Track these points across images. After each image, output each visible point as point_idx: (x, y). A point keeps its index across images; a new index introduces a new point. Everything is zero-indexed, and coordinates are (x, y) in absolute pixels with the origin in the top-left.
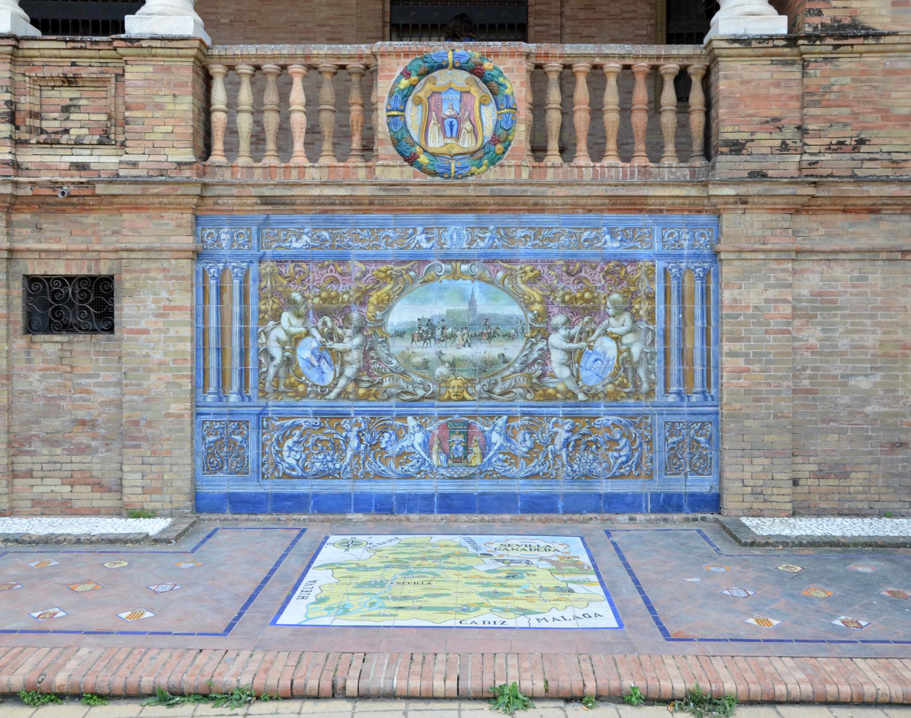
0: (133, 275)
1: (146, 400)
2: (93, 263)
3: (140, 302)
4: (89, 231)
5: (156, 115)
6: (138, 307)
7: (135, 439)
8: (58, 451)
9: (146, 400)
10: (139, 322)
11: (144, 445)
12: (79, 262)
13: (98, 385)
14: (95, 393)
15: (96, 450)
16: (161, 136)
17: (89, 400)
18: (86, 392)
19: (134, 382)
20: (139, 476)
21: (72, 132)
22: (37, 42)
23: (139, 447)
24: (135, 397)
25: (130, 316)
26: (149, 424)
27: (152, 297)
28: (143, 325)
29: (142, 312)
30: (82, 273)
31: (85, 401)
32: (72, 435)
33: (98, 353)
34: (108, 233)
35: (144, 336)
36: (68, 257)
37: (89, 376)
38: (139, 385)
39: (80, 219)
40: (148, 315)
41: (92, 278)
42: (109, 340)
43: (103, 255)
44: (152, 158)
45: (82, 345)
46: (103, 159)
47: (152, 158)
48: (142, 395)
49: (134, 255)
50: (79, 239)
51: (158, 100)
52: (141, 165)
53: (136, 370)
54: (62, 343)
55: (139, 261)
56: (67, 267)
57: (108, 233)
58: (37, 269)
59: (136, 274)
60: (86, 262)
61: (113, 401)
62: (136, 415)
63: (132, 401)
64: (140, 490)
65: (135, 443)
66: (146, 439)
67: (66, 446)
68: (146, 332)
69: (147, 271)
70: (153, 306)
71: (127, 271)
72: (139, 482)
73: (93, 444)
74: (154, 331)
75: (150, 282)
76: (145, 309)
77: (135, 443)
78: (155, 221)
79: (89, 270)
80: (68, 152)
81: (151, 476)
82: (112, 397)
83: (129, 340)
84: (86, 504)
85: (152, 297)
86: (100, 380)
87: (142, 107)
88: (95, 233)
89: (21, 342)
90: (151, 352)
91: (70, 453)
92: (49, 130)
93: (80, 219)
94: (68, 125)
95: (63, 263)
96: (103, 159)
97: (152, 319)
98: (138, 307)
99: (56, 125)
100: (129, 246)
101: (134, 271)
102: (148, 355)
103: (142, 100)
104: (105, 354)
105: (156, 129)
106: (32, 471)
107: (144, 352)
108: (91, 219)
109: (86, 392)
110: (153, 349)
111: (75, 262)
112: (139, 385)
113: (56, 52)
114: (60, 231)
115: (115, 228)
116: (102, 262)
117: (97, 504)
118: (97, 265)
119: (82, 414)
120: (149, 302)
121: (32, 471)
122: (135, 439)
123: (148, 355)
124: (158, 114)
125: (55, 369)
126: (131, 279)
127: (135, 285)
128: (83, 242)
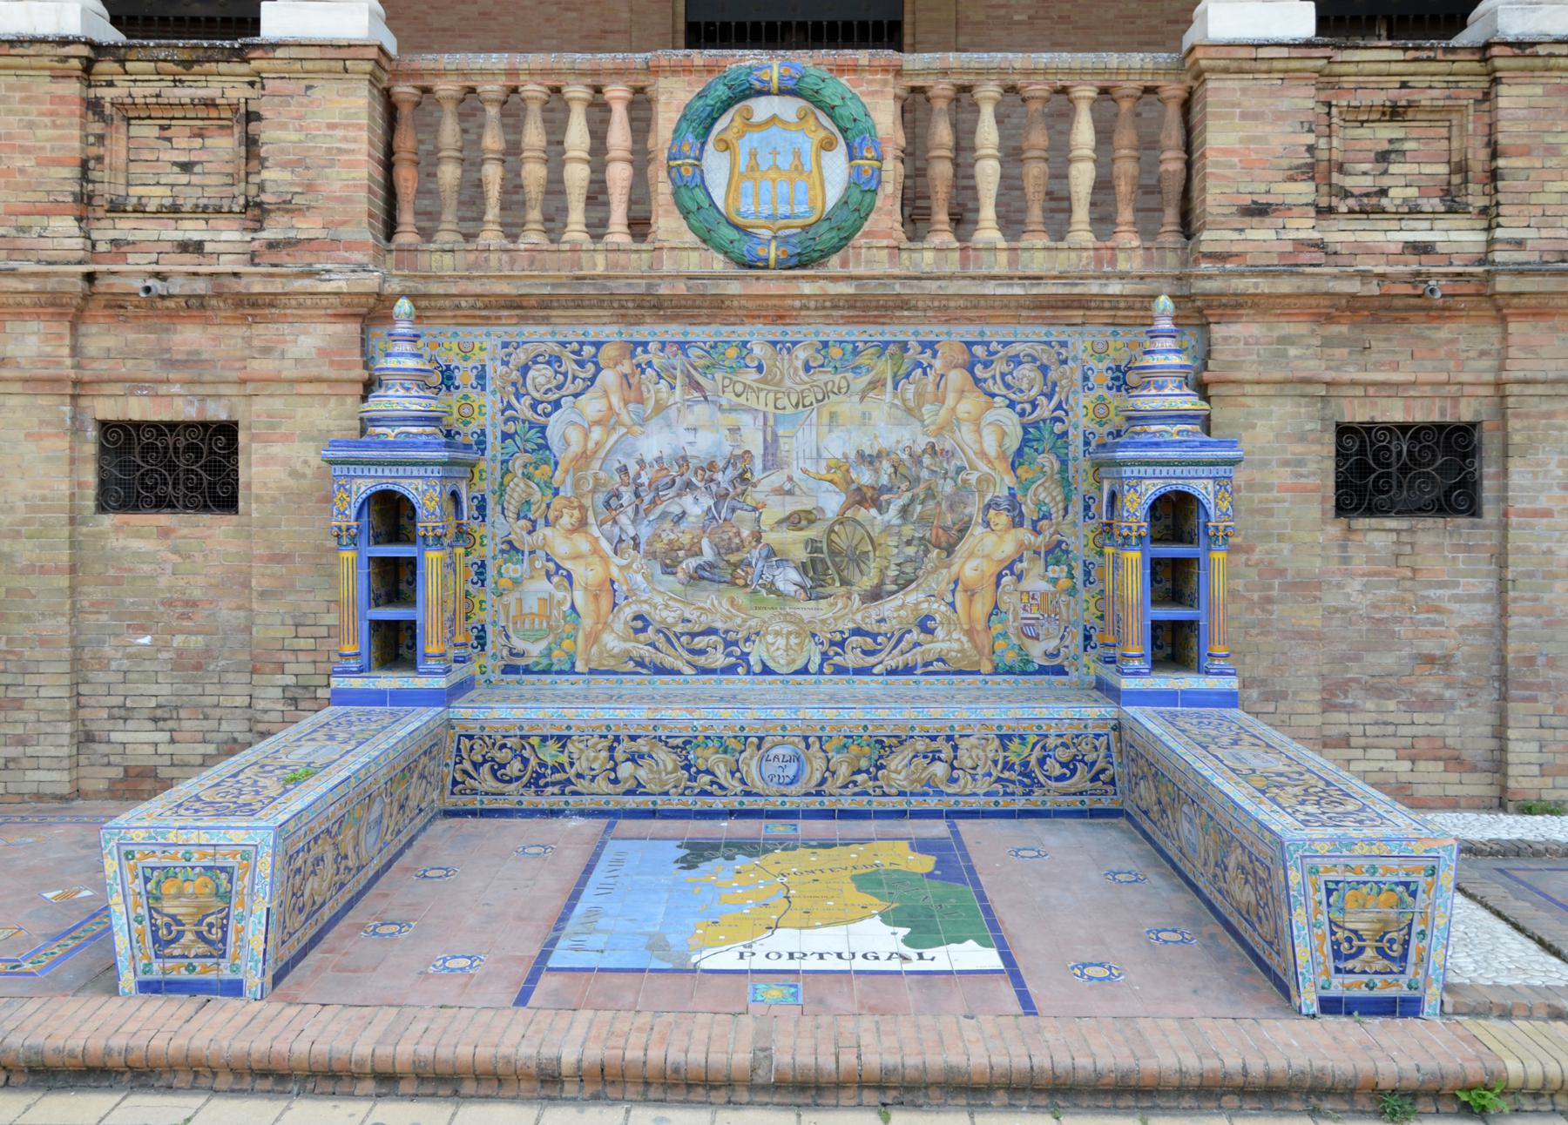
0: (1526, 422)
1: (1548, 624)
2: (1449, 403)
3: (1538, 465)
4: (1442, 352)
5: (1549, 164)
6: (1535, 474)
7: (1527, 686)
8: (1391, 705)
9: (1548, 624)
10: (1536, 499)
11: (1544, 696)
12: (1426, 401)
13: (1457, 599)
14: (1451, 612)
15: (1451, 705)
16: (1556, 198)
17: (1442, 624)
18: (1438, 610)
19: (1529, 595)
20: (1535, 746)
21: (1392, 193)
22: (1358, 52)
23: (1534, 699)
24: (1528, 620)
25: (1523, 488)
26: (1552, 663)
27: (1556, 458)
28: (1543, 503)
29: (1541, 481)
30: (1430, 419)
31: (1435, 624)
32: (1413, 679)
33: (1456, 548)
34: (1472, 354)
35: (1545, 521)
36: (1412, 393)
37: (1442, 585)
38: (1535, 600)
39: (1428, 333)
40: (1551, 487)
41: (1440, 427)
42: (1474, 526)
43: (1468, 390)
44: (1544, 233)
45: (1433, 539)
46: (1454, 236)
47: (1544, 233)
48: (1540, 616)
49: (1530, 390)
50: (1428, 364)
51: (1550, 139)
52: (1529, 244)
53: (1530, 575)
54: (1398, 532)
55: (1536, 399)
56: (1407, 409)
57: (1472, 354)
58: (1358, 414)
59: (1532, 421)
60: (1438, 402)
61: (1479, 625)
62: (1530, 648)
63: (1524, 625)
64: (1535, 770)
65: (1527, 693)
66: (1545, 686)
67: (1404, 697)
68: (1547, 513)
69: (1549, 415)
70: (1560, 472)
71: (1517, 416)
72: (1535, 757)
73: (1448, 694)
74: (1561, 512)
75: (1555, 433)
76: (1545, 476)
77: (1527, 693)
78: (1562, 335)
79: (1443, 414)
80: (1394, 225)
81: (1554, 748)
82: (1478, 619)
83: (1520, 527)
84: (1436, 791)
85: (1556, 458)
86: (1459, 591)
87: (1526, 152)
88: (1451, 355)
89: (1335, 529)
90: (1555, 547)
91: (1410, 708)
92: (1356, 191)
93: (1428, 333)
94: (1385, 182)
95: (1399, 403)
96: (1454, 236)
97: (1557, 492)
98: (1535, 474)
99: (1367, 182)
100: (1530, 375)
101: (1527, 416)
102: (1550, 552)
103: (1526, 141)
104: (1468, 548)
105: (1549, 187)
106: (1348, 736)
107: (1544, 546)
108: (1445, 331)
109: (1438, 610)
110: (1559, 541)
111: (1420, 401)
112: (1535, 600)
113: (1384, 67)
114: (1395, 352)
115: (1484, 347)
116: (1463, 401)
117: (1452, 791)
118: (1455, 406)
119: (1429, 647)
120: (1552, 466)
121: (1348, 736)
122: (1527, 686)
123: (1550, 552)
124: (1552, 162)
125: (1387, 574)
126: (1524, 428)
127: (1529, 438)
128: (1435, 370)
